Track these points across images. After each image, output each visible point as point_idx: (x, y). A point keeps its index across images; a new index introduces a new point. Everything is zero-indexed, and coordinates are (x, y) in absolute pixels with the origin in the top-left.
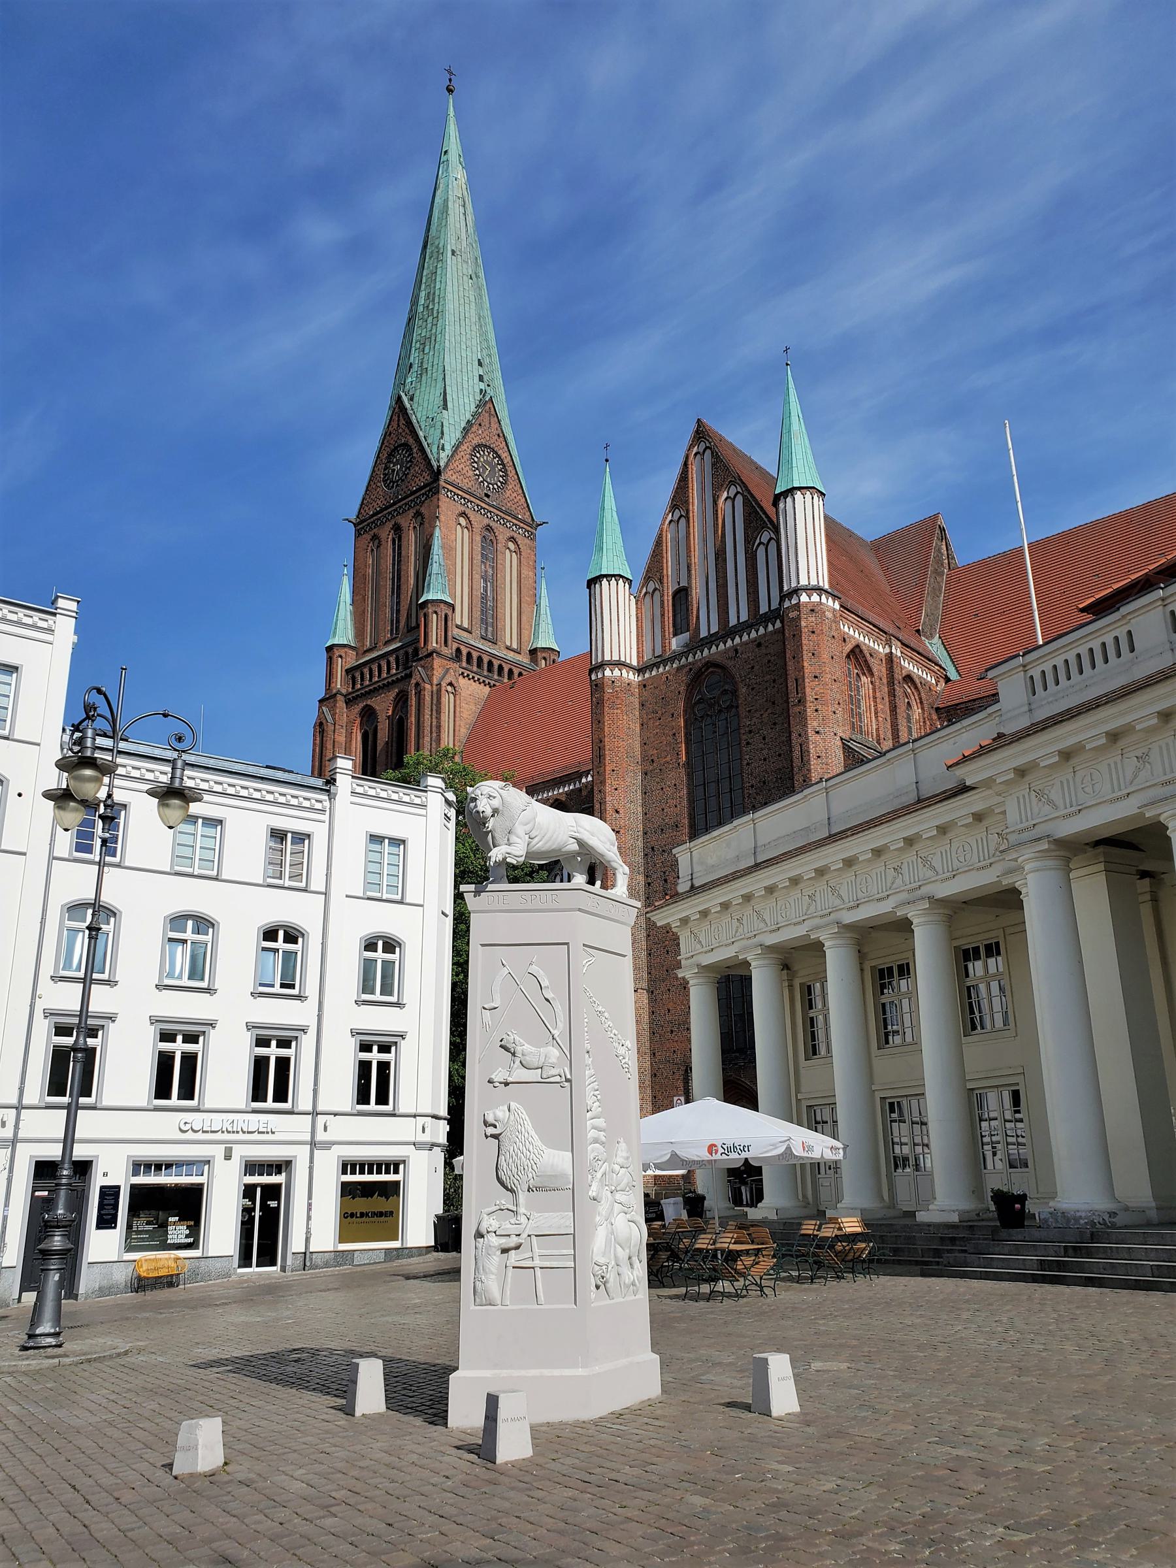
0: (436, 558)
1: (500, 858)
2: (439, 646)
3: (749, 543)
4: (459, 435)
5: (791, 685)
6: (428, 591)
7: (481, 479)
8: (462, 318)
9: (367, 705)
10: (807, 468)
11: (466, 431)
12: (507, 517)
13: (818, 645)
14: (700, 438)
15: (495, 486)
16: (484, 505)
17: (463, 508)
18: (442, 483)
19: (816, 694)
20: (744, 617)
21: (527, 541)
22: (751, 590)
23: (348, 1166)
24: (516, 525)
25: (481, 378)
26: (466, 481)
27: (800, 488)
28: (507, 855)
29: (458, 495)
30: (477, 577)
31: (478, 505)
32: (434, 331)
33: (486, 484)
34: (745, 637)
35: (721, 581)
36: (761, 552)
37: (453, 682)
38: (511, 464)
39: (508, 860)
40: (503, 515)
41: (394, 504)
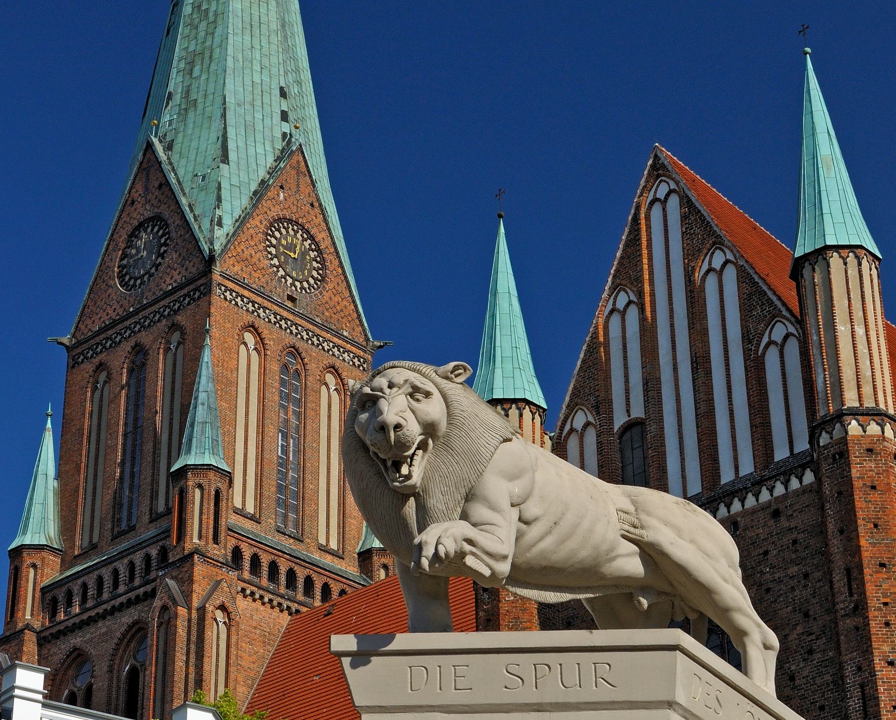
0: (202, 396)
1: (449, 547)
2: (203, 543)
3: (750, 342)
4: (245, 201)
5: (839, 578)
6: (189, 451)
7: (281, 272)
8: (255, 23)
9: (75, 649)
10: (847, 215)
12: (324, 334)
13: (883, 508)
14: (658, 176)
15: (305, 285)
16: (285, 314)
17: (250, 318)
18: (216, 277)
19: (885, 596)
20: (747, 467)
22: (758, 421)
24: (339, 347)
25: (284, 116)
26: (256, 275)
27: (837, 248)
28: (468, 548)
29: (242, 296)
30: (271, 430)
31: (275, 314)
32: (208, 43)
33: (290, 281)
34: (750, 501)
35: (703, 407)
36: (772, 359)
37: (227, 604)
38: (332, 250)
39: (470, 561)
40: (318, 331)
41: (136, 312)
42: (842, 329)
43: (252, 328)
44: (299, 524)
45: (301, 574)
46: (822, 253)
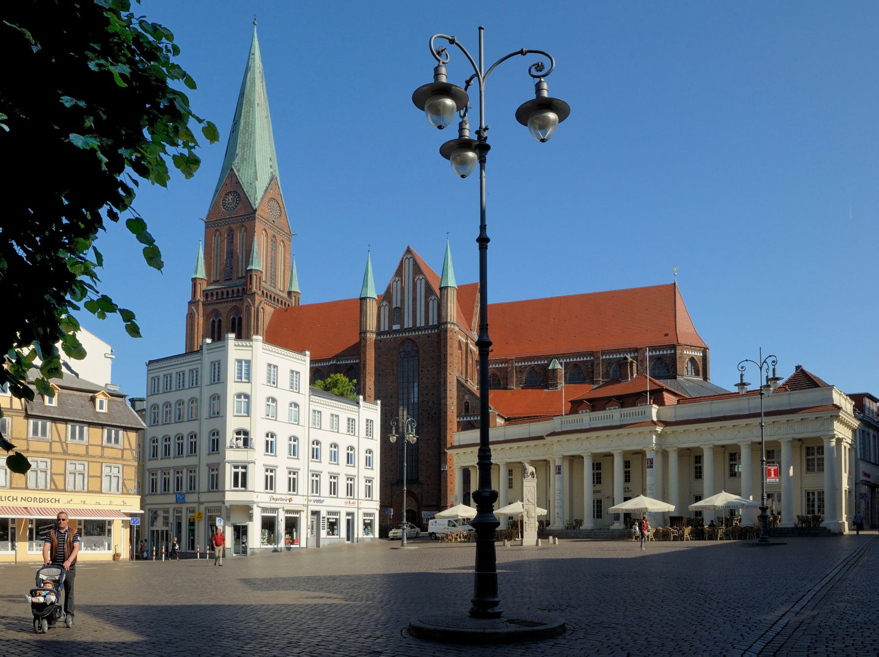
0: (255, 250)
6: (252, 264)
11: (266, 191)
18: (257, 215)
20: (423, 325)
21: (288, 242)
23: (365, 514)
34: (423, 332)
36: (431, 303)
42: (449, 304)
43: (265, 230)
44: (275, 283)
45: (276, 298)
46: (447, 287)
